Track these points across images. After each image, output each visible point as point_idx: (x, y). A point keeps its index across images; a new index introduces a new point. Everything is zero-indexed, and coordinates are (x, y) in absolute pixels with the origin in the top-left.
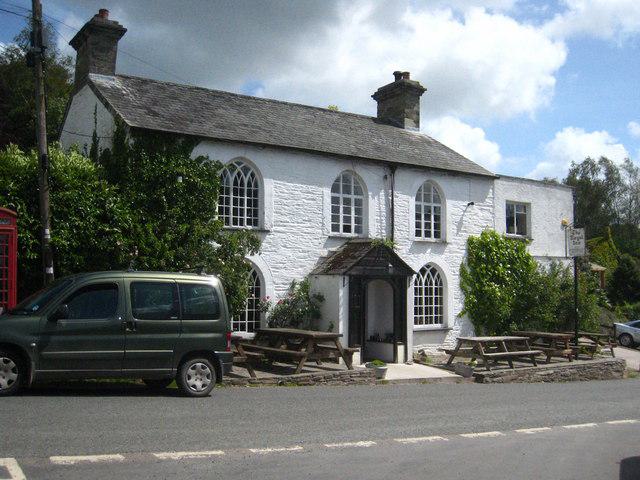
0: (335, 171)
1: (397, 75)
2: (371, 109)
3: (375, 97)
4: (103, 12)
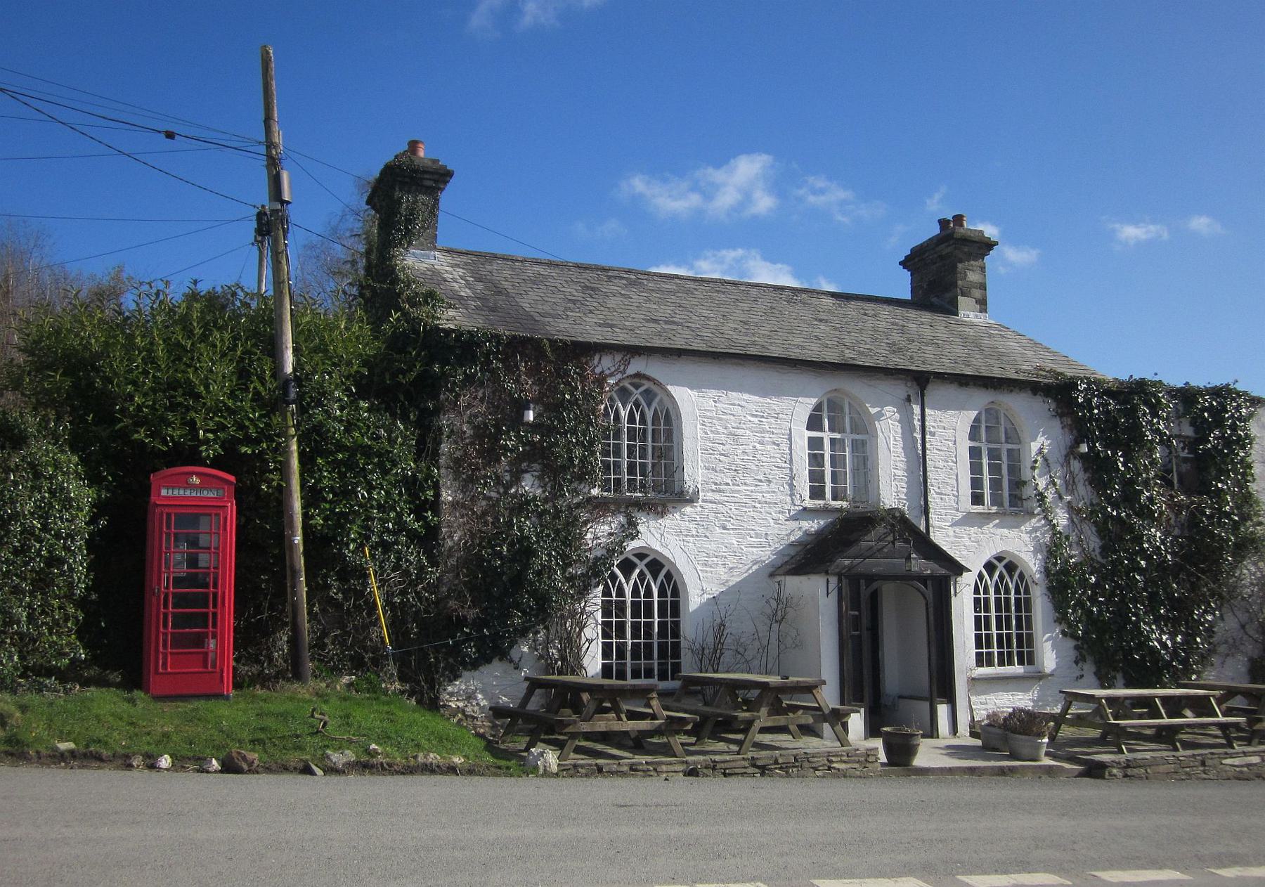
0: (983, 398)
1: (943, 223)
2: (901, 285)
3: (905, 264)
4: (958, 219)
